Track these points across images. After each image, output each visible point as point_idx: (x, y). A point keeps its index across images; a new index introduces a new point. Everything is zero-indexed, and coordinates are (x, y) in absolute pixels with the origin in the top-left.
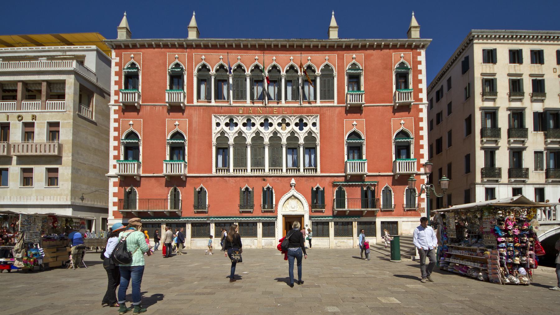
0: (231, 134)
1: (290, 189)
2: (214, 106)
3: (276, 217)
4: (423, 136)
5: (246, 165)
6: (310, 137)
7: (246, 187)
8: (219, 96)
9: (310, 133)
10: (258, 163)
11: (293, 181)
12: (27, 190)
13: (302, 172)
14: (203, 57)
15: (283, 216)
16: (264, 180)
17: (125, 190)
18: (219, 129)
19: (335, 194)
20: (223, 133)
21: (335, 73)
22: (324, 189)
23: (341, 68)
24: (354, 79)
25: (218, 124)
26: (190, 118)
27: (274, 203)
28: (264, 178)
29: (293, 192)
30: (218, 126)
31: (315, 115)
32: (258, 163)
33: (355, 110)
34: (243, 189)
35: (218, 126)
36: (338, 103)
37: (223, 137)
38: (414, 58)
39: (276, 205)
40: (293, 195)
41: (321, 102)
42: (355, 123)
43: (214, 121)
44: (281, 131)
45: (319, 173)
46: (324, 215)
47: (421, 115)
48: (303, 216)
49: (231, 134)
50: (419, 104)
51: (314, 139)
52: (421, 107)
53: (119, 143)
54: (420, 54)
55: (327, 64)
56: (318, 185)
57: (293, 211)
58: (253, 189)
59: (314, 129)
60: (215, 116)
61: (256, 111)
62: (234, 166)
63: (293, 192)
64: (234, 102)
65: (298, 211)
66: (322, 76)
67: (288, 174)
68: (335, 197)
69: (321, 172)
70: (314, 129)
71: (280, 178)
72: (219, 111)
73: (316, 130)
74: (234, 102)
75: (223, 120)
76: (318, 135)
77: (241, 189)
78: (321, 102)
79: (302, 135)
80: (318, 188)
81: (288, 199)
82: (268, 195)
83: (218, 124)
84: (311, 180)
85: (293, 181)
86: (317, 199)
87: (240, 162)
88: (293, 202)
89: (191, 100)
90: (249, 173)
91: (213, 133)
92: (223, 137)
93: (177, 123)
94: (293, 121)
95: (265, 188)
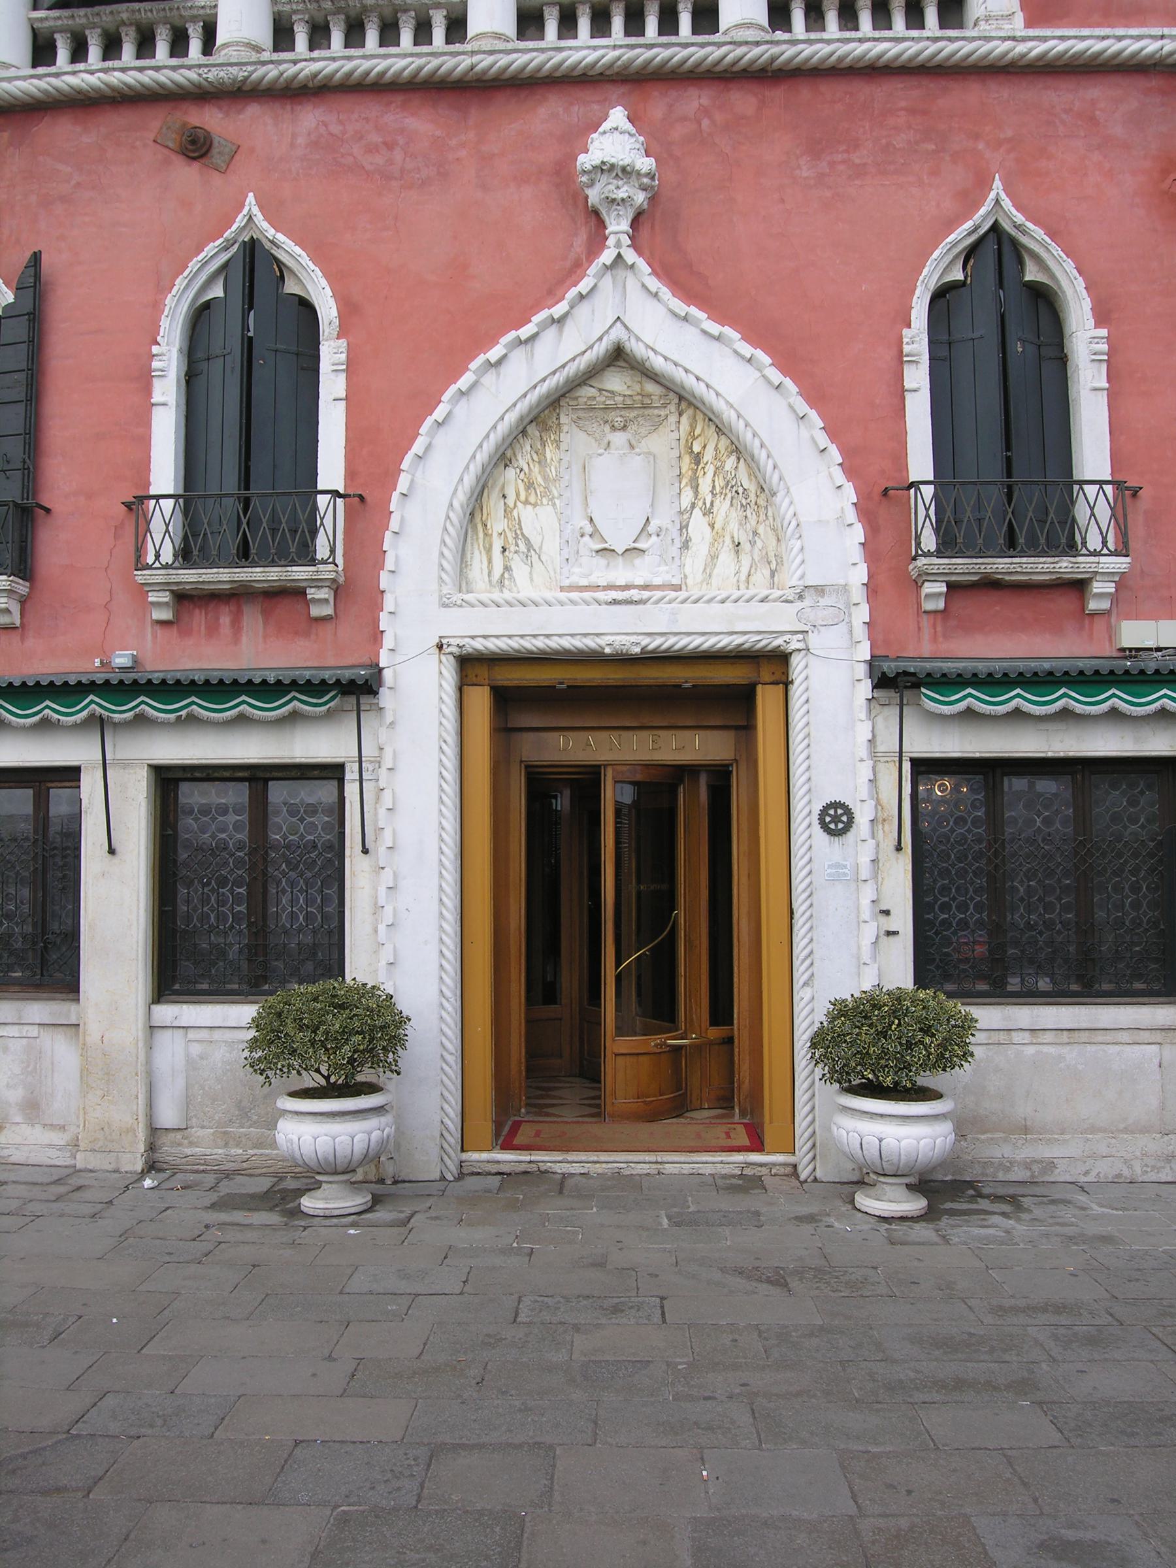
1: (575, 270)
3: (360, 689)
11: (615, 140)
15: (471, 666)
16: (197, 147)
27: (331, 470)
39: (366, 503)
40: (618, 356)
48: (773, 664)
57: (625, 597)
65: (697, 606)
71: (420, 123)
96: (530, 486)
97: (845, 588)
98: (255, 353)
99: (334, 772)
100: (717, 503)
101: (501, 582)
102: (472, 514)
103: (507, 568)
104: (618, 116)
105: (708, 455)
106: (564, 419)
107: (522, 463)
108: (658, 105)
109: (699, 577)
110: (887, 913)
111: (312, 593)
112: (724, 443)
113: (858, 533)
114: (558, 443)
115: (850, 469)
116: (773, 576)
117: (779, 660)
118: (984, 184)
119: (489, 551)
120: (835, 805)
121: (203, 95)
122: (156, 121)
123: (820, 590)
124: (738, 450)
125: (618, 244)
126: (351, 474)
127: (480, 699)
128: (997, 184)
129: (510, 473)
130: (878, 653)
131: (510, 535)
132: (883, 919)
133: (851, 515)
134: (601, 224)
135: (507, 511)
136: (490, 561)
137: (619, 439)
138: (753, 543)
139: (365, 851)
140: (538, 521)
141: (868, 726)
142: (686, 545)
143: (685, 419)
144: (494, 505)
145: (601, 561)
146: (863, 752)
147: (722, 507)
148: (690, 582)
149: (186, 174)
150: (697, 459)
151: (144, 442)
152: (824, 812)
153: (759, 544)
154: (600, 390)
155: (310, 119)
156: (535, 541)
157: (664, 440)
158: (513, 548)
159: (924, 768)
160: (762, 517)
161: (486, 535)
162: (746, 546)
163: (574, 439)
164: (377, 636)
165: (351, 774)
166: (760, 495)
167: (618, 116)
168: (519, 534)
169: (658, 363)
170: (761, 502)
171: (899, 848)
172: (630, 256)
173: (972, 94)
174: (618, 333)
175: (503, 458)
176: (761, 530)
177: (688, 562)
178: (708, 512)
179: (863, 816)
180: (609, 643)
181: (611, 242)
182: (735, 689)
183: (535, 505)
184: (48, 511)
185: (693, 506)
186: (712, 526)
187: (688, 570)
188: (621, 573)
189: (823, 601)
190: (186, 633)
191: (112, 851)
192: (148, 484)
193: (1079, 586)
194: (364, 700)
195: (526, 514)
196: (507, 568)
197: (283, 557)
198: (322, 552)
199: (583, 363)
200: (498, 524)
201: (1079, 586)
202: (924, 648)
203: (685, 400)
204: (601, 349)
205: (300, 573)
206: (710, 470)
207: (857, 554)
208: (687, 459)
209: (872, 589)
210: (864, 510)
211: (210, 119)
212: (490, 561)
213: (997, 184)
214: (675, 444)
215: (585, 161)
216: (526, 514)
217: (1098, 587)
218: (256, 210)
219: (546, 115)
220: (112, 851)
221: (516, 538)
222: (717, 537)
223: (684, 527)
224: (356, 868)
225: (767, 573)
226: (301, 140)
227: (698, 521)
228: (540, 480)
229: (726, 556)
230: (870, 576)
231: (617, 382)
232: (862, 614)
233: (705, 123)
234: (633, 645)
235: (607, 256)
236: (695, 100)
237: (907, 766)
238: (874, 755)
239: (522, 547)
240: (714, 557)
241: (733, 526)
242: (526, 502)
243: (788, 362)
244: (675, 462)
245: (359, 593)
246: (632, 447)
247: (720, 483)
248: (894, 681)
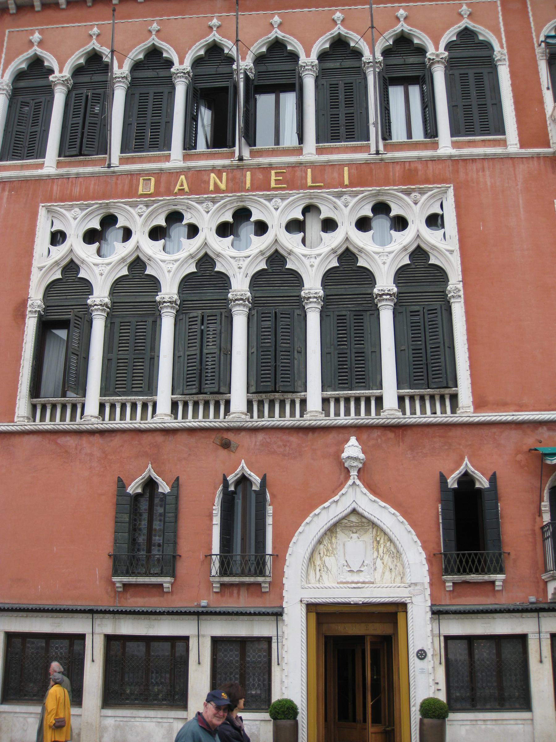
0: (101, 271)
1: (341, 485)
2: (50, 179)
5: (151, 388)
6: (420, 272)
7: (145, 475)
9: (419, 254)
10: (202, 379)
15: (311, 607)
16: (226, 445)
18: (59, 252)
19: (546, 505)
20: (71, 267)
22: (493, 479)
25: (58, 237)
28: (225, 439)
29: (355, 496)
31: (436, 188)
32: (202, 379)
34: (134, 487)
36: (522, 147)
39: (279, 558)
44: (300, 250)
46: (504, 601)
48: (403, 606)
49: (101, 271)
51: (440, 275)
55: (466, 29)
56: (467, 465)
57: (358, 585)
58: (176, 485)
59: (432, 237)
60: (49, 211)
61: (198, 184)
62: (104, 391)
65: (379, 589)
66: (451, 65)
67: (332, 420)
68: (547, 518)
69: (480, 404)
70: (432, 237)
71: (294, 439)
75: (76, 221)
77: (121, 485)
78: (455, 145)
80: (467, 480)
82: (242, 507)
85: (353, 449)
86: (467, 530)
87: (130, 374)
88: (354, 547)
90: (163, 416)
91: (34, 270)
95: (231, 478)
96: (328, 550)
97: (423, 584)
98: (242, 507)
99: (269, 640)
100: (384, 556)
101: (319, 581)
102: (310, 559)
103: (321, 576)
104: (353, 440)
105: (382, 541)
106: (338, 530)
107: (325, 543)
108: (365, 436)
109: (379, 579)
110: (437, 683)
111: (263, 585)
112: (386, 538)
113: (426, 567)
114: (336, 537)
115: (424, 548)
116: (402, 579)
117: (404, 605)
118: (462, 459)
119: (315, 570)
120: (421, 650)
121: (228, 429)
122: (213, 436)
123: (416, 584)
124: (390, 540)
125: (354, 479)
126: (274, 548)
127: (313, 616)
128: (466, 459)
129: (322, 546)
130: (434, 603)
131: (322, 566)
132: (436, 685)
133: (424, 562)
134: (349, 472)
135: (321, 558)
136: (316, 574)
137: (355, 536)
138: (395, 569)
139: (278, 664)
140: (330, 561)
141: (430, 626)
142: (375, 569)
143: (374, 530)
144: (317, 557)
145: (349, 574)
146: (429, 634)
147: (386, 557)
148: (377, 581)
149: (223, 453)
150: (378, 542)
151: (210, 535)
152: (418, 652)
153: (397, 569)
154: (349, 521)
155: (260, 437)
156: (329, 568)
157: (368, 537)
158: (323, 570)
159: (448, 638)
160: (398, 560)
161: (314, 565)
162: (393, 570)
163: (341, 536)
164: (282, 598)
165: (274, 640)
166: (397, 554)
167: (353, 440)
168: (324, 565)
169: (366, 514)
170: (398, 556)
171: (440, 663)
172: (358, 482)
173: (458, 432)
174: (354, 505)
175: (320, 542)
176: (398, 564)
177: (376, 574)
178: (382, 559)
179: (429, 654)
180: (353, 600)
181: (352, 477)
182: (392, 614)
183: (329, 556)
184: (180, 556)
185: (377, 557)
186: (383, 563)
187: (376, 577)
188: (356, 578)
189: (417, 588)
190: (223, 596)
191: (199, 663)
192: (211, 549)
193: (493, 583)
194: (279, 617)
195: (326, 559)
196: (321, 576)
197: (256, 575)
198: (267, 573)
199: (344, 514)
200: (318, 562)
201: (493, 583)
202: (447, 602)
203: (374, 525)
204: (349, 510)
205: (260, 579)
206: (382, 546)
207: (426, 574)
208: (375, 542)
209: (431, 584)
210: (429, 560)
211: (230, 436)
212: (316, 574)
213: (466, 459)
214: (371, 538)
215: (344, 455)
216: (326, 559)
217: (497, 583)
218: (244, 465)
219: (331, 437)
220: (199, 663)
221: (323, 566)
222: (385, 567)
223: (375, 563)
224: (276, 671)
225: (400, 578)
226: (258, 443)
227: (379, 562)
228: (331, 549)
229: (387, 573)
230: (431, 580)
231: (353, 518)
232: (428, 592)
233: (379, 440)
234: (360, 601)
235: (350, 482)
236: (376, 433)
237: (442, 638)
238: (433, 635)
239: (325, 569)
240: (384, 573)
241: (390, 563)
242: (327, 555)
243: (405, 514)
244: (372, 544)
245: (277, 585)
246: (359, 538)
247: (385, 550)
248: (438, 613)
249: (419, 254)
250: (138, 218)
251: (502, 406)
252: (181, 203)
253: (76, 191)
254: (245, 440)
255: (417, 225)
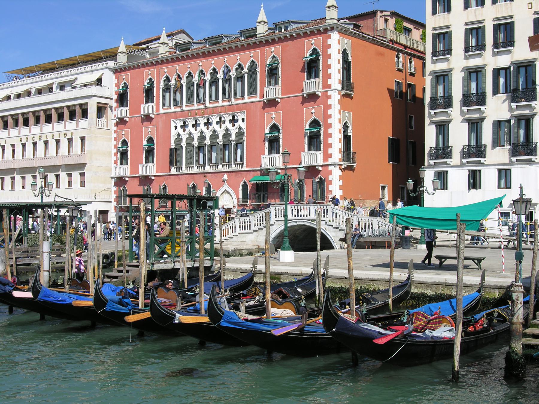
0: (184, 136)
4: (331, 124)
6: (240, 134)
8: (176, 103)
11: (225, 177)
12: (70, 190)
13: (233, 168)
14: (166, 70)
17: (120, 188)
20: (179, 135)
21: (258, 69)
23: (263, 61)
24: (273, 72)
25: (176, 128)
26: (157, 124)
29: (226, 187)
30: (175, 130)
33: (272, 103)
34: (191, 186)
35: (175, 130)
36: (260, 98)
37: (179, 139)
38: (325, 42)
41: (249, 98)
42: (274, 116)
43: (173, 125)
45: (245, 168)
47: (330, 102)
49: (184, 136)
50: (328, 91)
52: (329, 93)
53: (117, 150)
54: (329, 37)
56: (244, 180)
63: (226, 187)
64: (187, 106)
69: (247, 166)
72: (175, 116)
73: (243, 125)
74: (187, 106)
76: (245, 131)
77: (188, 185)
78: (249, 98)
79: (233, 131)
81: (223, 193)
83: (176, 128)
84: (239, 174)
85: (225, 177)
89: (158, 110)
92: (179, 139)
93: (149, 130)
94: (228, 118)
249: (240, 128)
250: (190, 122)
251: (251, 166)
252: (197, 117)
253: (178, 116)
254: (208, 175)
255: (240, 121)
